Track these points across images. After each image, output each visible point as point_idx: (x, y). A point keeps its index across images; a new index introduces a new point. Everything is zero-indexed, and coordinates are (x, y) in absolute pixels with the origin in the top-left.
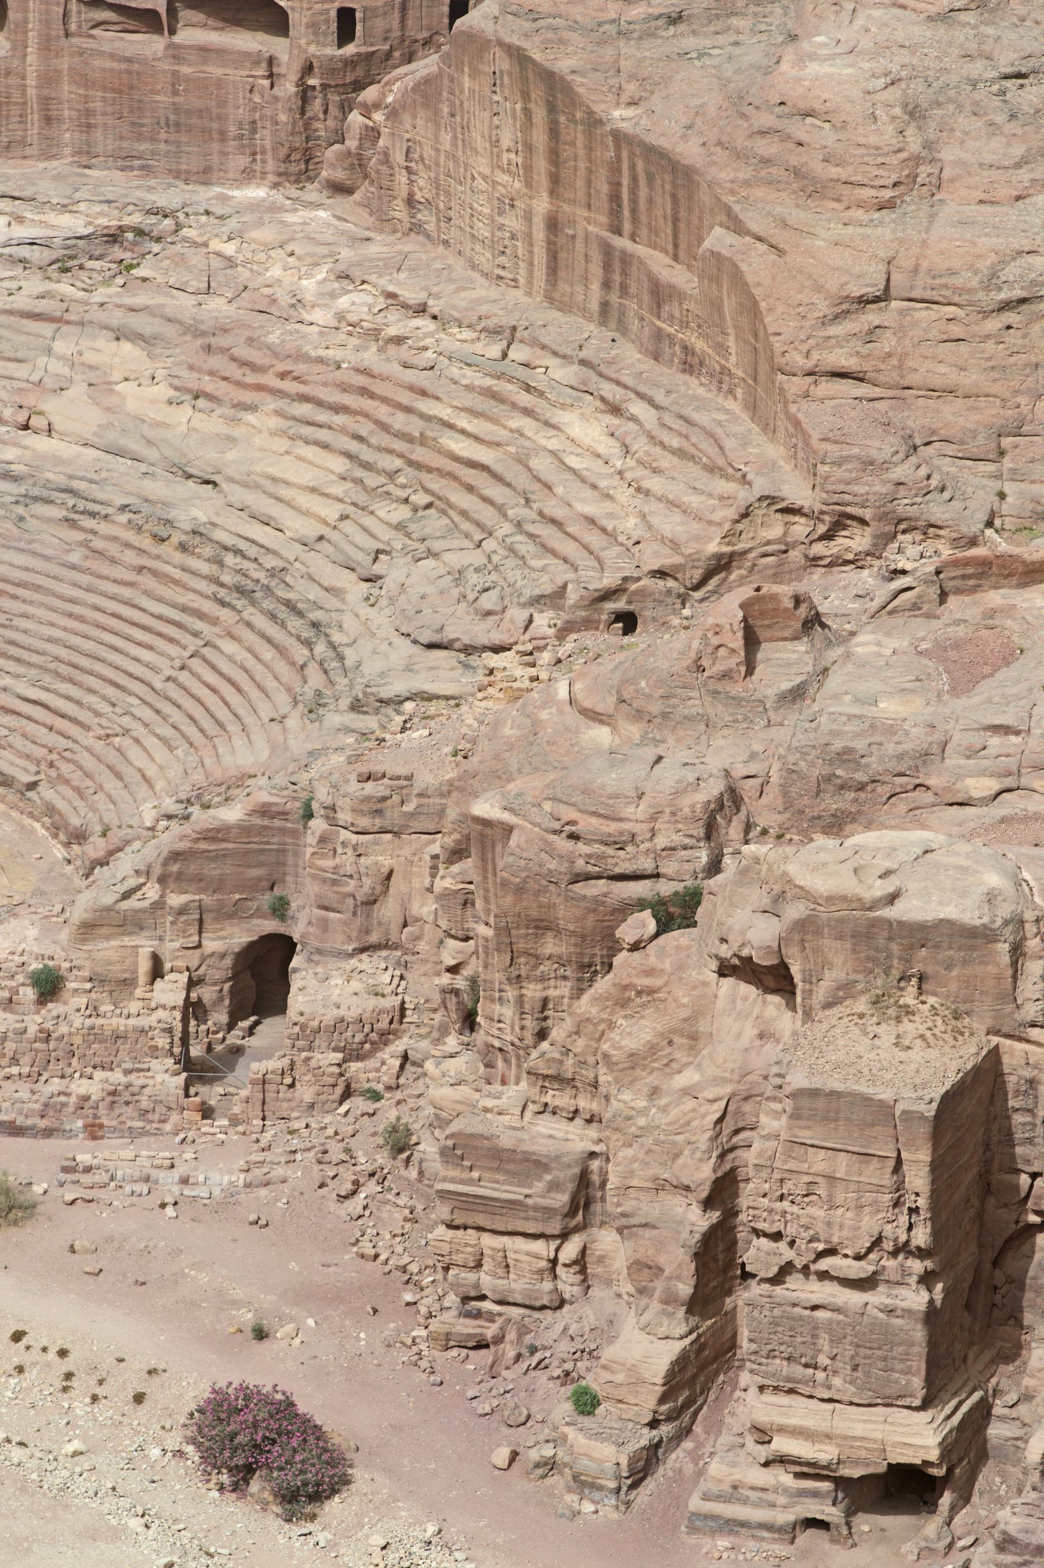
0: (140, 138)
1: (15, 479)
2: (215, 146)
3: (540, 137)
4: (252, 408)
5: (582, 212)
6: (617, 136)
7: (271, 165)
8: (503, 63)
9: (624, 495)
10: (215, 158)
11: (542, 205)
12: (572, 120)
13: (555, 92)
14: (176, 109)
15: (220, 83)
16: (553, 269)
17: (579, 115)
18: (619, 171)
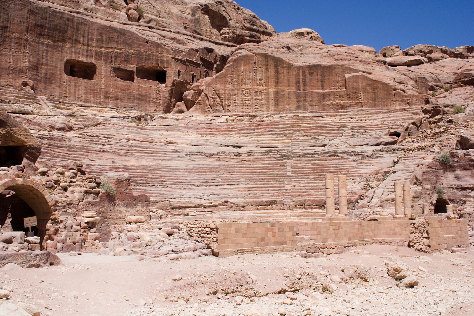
0: (130, 102)
1: (179, 152)
2: (147, 104)
3: (272, 72)
4: (228, 134)
5: (286, 89)
6: (298, 68)
7: (162, 108)
8: (258, 59)
9: (368, 121)
10: (148, 108)
11: (272, 90)
12: (283, 67)
13: (278, 62)
14: (139, 95)
15: (150, 88)
16: (277, 103)
17: (285, 65)
18: (299, 76)
